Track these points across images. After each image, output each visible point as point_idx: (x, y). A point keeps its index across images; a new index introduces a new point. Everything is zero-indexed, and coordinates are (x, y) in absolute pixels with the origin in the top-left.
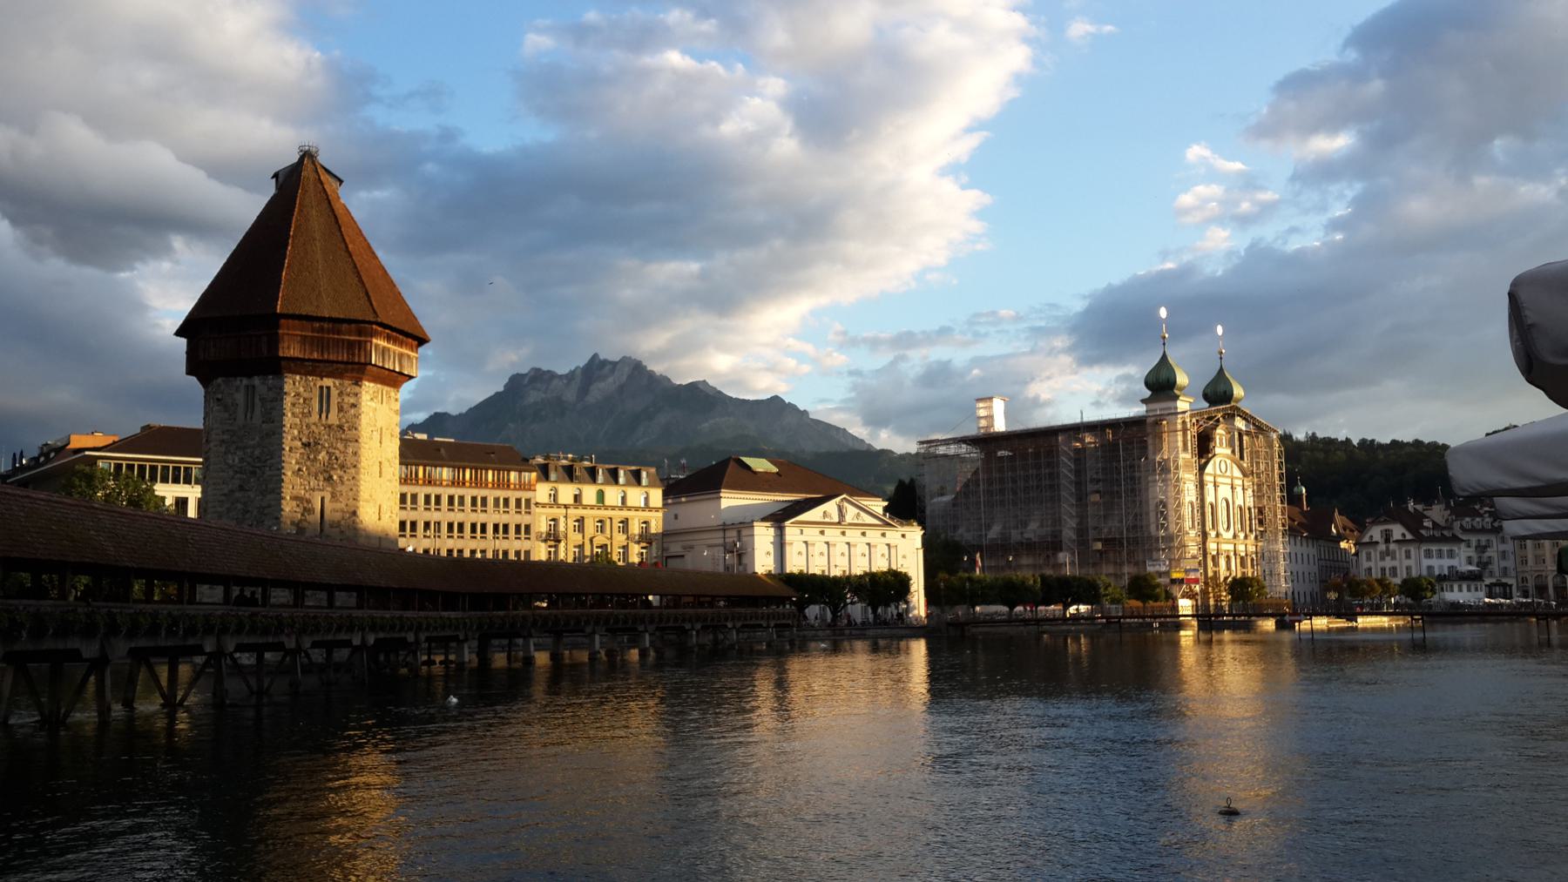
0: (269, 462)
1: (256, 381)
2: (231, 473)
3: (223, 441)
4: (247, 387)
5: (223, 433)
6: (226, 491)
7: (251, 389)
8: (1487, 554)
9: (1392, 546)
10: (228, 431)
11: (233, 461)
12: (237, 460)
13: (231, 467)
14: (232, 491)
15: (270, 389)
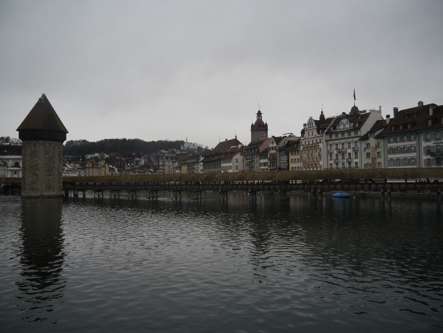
0: (54, 158)
1: (51, 142)
2: (46, 159)
3: (44, 153)
4: (49, 143)
5: (44, 151)
6: (45, 163)
7: (50, 144)
8: (80, 174)
9: (65, 171)
10: (45, 151)
11: (47, 157)
12: (47, 157)
13: (46, 158)
14: (47, 163)
15: (54, 144)
